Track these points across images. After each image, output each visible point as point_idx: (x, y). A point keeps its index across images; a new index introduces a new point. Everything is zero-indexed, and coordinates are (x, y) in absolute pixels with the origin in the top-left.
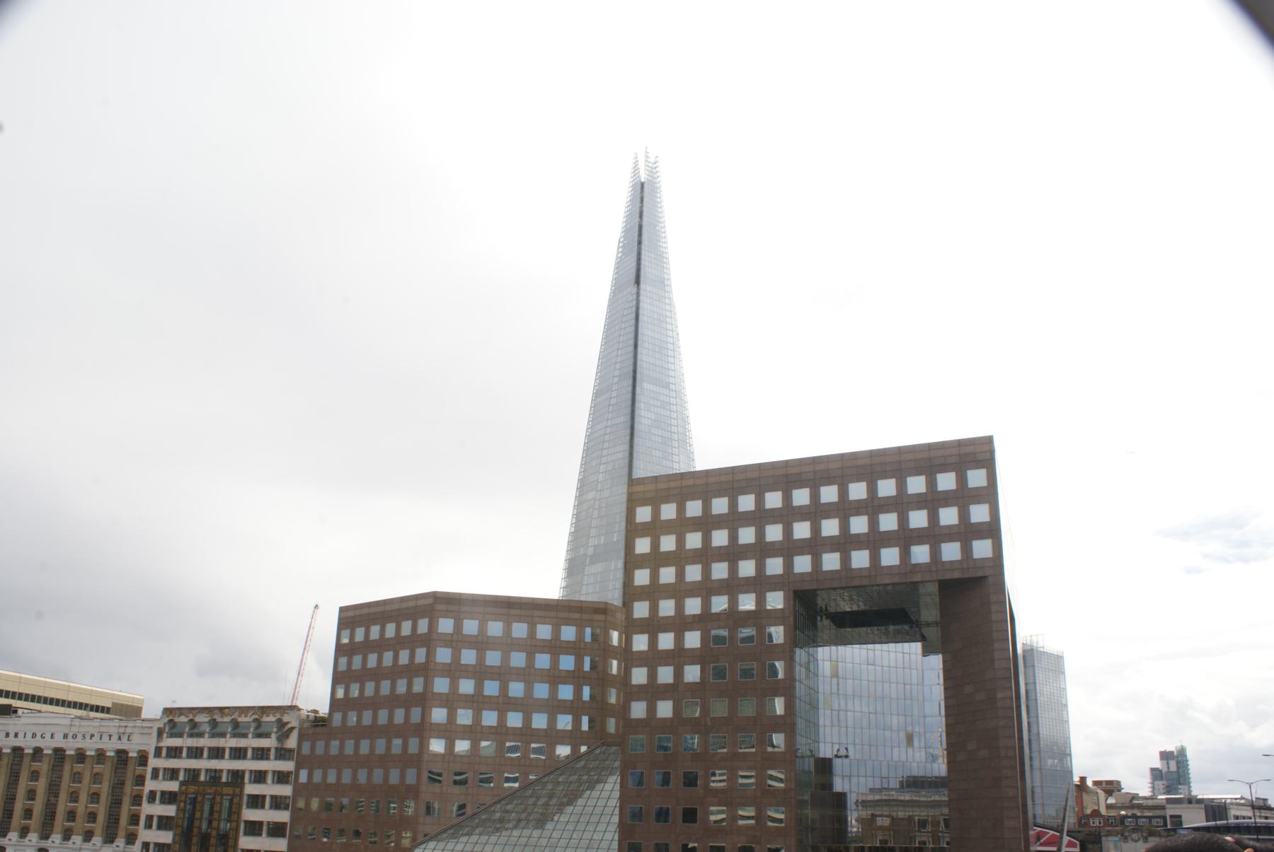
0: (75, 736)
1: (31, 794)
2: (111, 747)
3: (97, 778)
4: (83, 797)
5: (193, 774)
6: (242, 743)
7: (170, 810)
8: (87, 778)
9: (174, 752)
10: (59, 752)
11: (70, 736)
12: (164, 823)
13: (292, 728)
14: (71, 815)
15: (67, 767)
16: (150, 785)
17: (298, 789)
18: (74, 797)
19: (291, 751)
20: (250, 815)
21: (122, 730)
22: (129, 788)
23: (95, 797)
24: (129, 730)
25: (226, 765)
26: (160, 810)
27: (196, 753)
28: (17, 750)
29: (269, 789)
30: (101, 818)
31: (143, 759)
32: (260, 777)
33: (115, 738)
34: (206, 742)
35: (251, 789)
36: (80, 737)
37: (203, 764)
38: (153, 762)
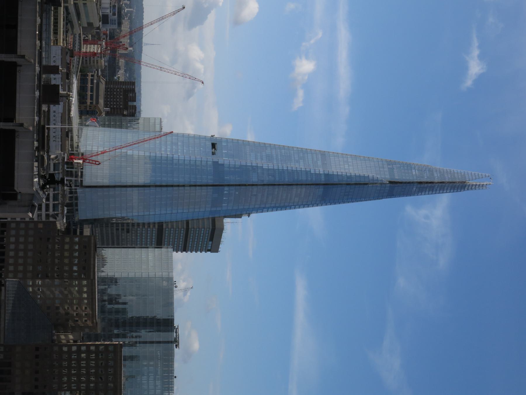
0: (54, 116)
6: (51, 199)
11: (55, 114)
13: (56, 219)
19: (49, 219)
21: (57, 137)
24: (57, 140)
33: (54, 134)
36: (54, 118)
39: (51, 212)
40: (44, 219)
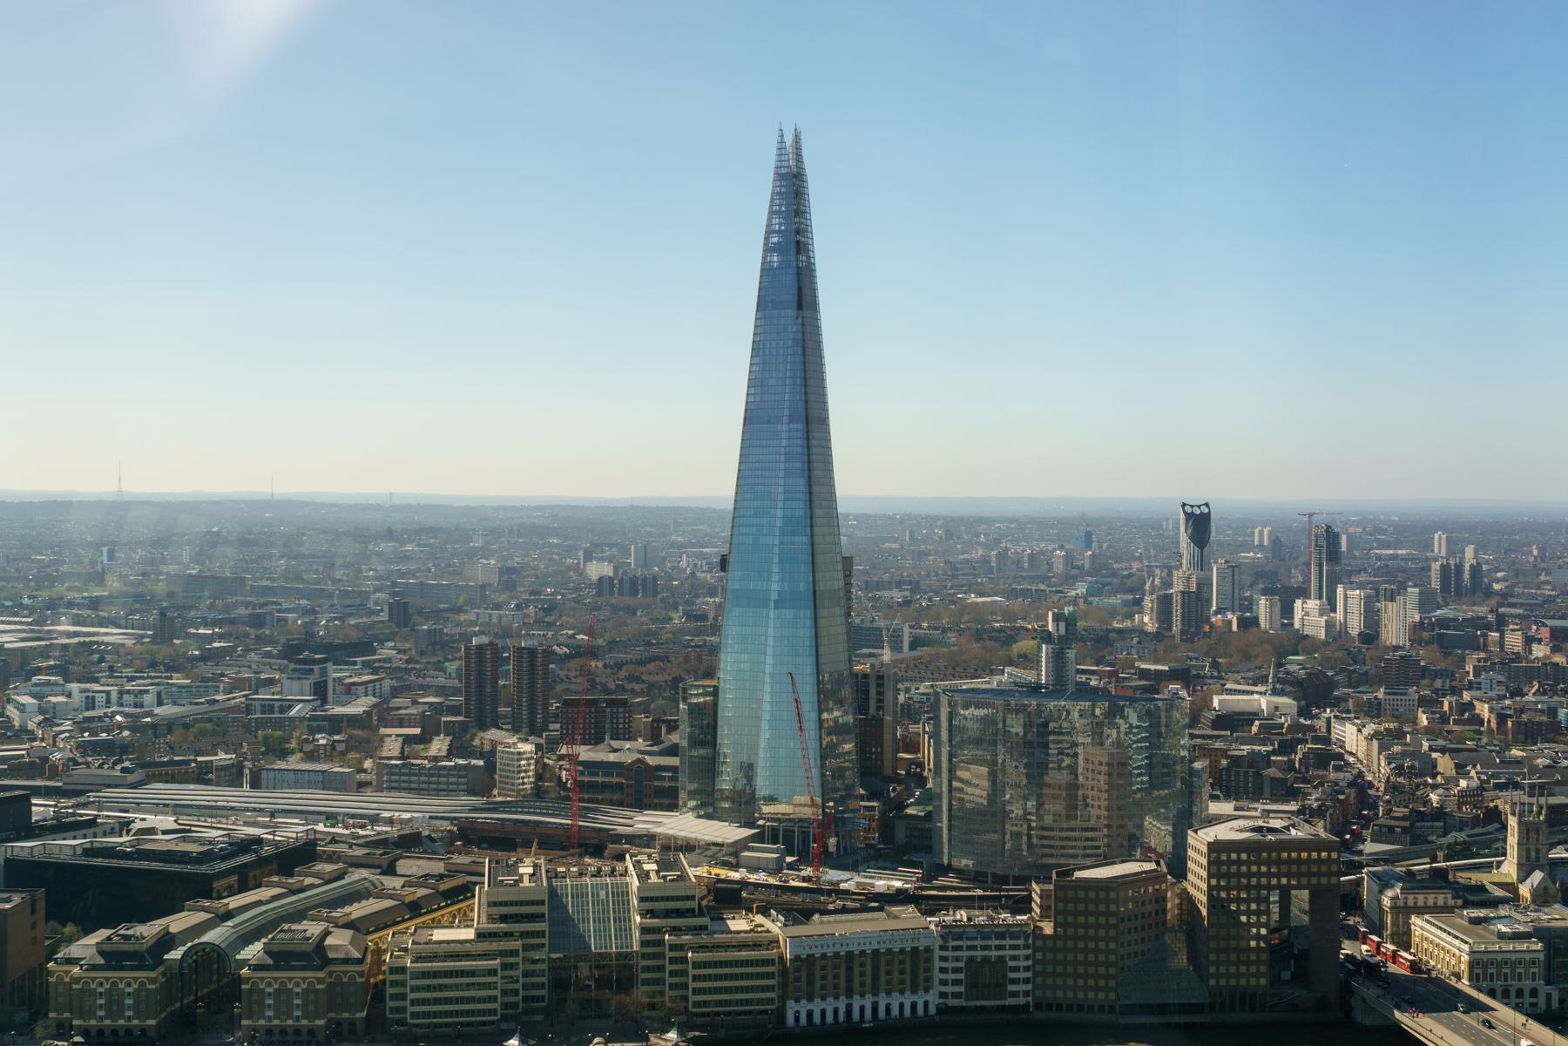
1: (862, 974)
2: (908, 946)
3: (902, 962)
4: (896, 973)
5: (971, 960)
7: (961, 976)
8: (896, 963)
9: (956, 948)
10: (876, 952)
12: (956, 982)
14: (888, 983)
15: (882, 959)
16: (938, 964)
17: (1036, 962)
18: (889, 973)
20: (1012, 975)
22: (922, 965)
23: (902, 972)
25: (994, 953)
26: (951, 976)
27: (973, 948)
28: (850, 954)
29: (1023, 963)
30: (908, 982)
31: (928, 950)
32: (1014, 958)
34: (978, 943)
35: (1011, 964)
37: (979, 953)
38: (938, 953)
39: (1021, 942)
40: (1029, 952)
